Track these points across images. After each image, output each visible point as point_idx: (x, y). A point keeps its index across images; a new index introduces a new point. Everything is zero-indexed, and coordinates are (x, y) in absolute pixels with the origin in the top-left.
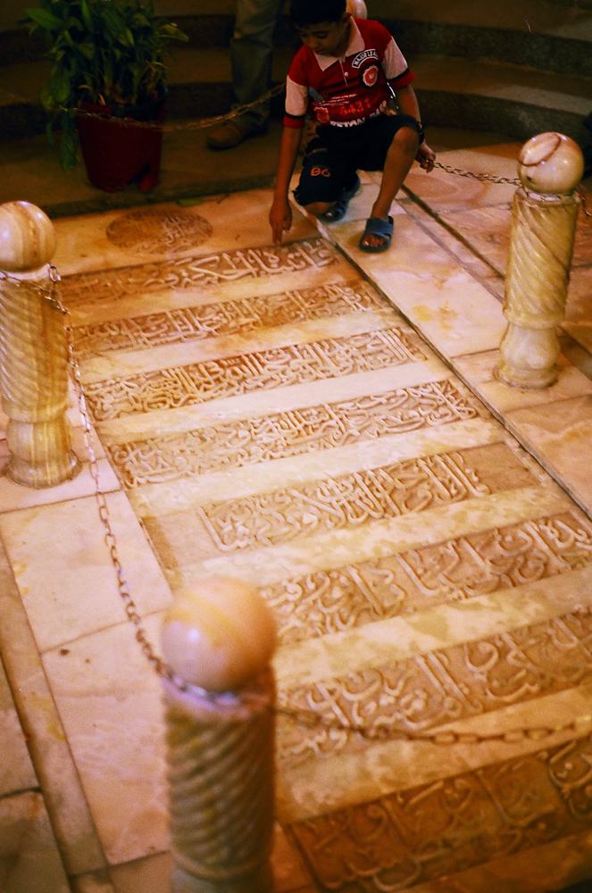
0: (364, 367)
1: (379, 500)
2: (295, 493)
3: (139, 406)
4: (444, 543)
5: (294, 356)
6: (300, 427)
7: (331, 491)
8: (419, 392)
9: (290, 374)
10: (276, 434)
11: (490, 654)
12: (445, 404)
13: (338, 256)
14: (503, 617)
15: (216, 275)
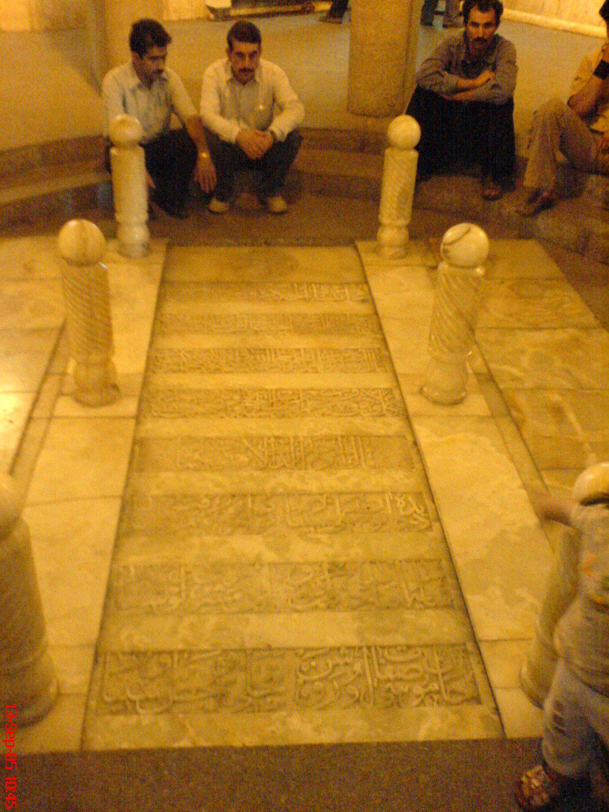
0: (342, 371)
3: (182, 368)
5: (301, 356)
6: (275, 400)
7: (269, 444)
10: (257, 403)
11: (309, 574)
12: (380, 404)
14: (330, 551)
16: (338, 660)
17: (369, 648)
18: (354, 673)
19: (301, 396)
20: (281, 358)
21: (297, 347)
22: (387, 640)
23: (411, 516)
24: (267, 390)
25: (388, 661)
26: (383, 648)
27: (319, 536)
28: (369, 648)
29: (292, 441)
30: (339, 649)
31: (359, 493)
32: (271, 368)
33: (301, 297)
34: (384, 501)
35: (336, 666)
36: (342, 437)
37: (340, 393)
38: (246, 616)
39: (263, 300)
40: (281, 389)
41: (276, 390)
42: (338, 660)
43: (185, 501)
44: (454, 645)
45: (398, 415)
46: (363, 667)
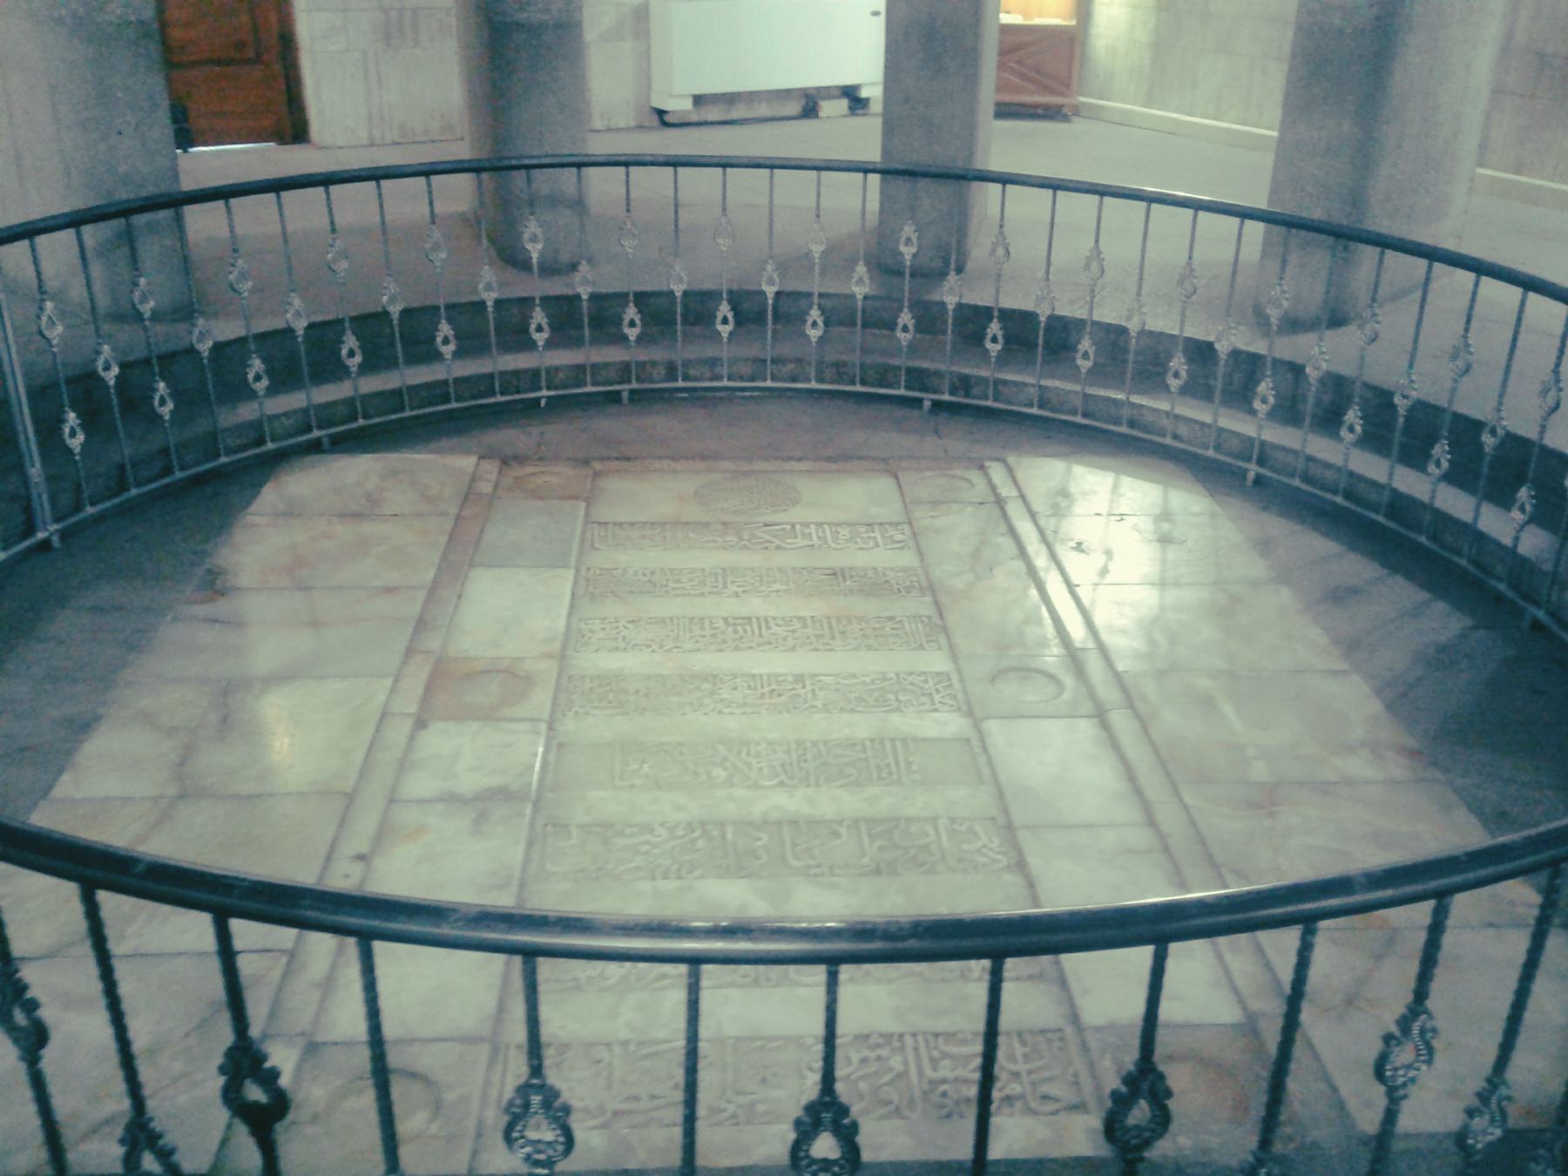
0: (869, 648)
1: (801, 769)
2: (721, 748)
4: (840, 822)
6: (767, 689)
8: (911, 679)
9: (791, 642)
13: (911, 543)
15: (777, 542)
16: (866, 1053)
17: (914, 1035)
18: (891, 1069)
19: (808, 682)
20: (775, 629)
21: (801, 614)
22: (942, 1025)
23: (979, 851)
24: (754, 676)
25: (945, 1055)
26: (937, 1035)
27: (835, 879)
28: (914, 1035)
29: (793, 746)
30: (868, 1036)
31: (898, 820)
32: (759, 645)
33: (806, 542)
34: (937, 830)
35: (864, 1061)
36: (873, 741)
37: (868, 680)
38: (725, 991)
39: (745, 547)
40: (777, 675)
41: (769, 676)
42: (866, 1053)
43: (628, 831)
44: (1043, 1032)
45: (959, 709)
46: (905, 1062)
